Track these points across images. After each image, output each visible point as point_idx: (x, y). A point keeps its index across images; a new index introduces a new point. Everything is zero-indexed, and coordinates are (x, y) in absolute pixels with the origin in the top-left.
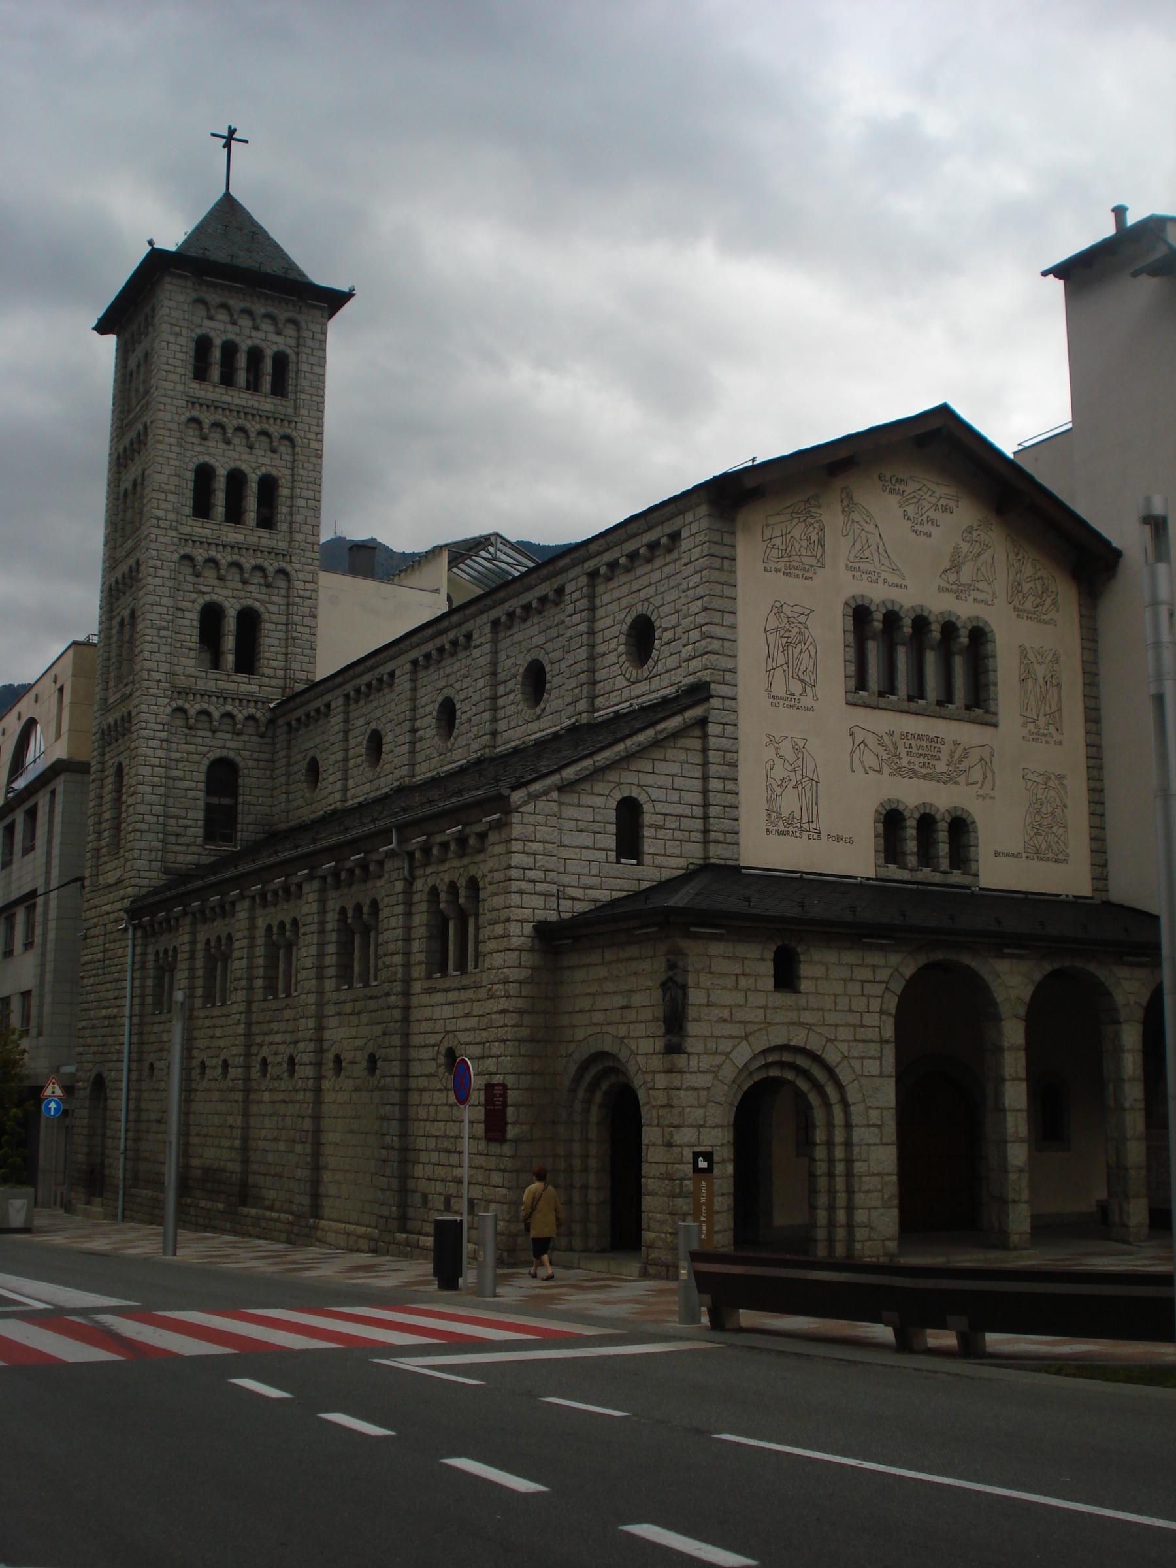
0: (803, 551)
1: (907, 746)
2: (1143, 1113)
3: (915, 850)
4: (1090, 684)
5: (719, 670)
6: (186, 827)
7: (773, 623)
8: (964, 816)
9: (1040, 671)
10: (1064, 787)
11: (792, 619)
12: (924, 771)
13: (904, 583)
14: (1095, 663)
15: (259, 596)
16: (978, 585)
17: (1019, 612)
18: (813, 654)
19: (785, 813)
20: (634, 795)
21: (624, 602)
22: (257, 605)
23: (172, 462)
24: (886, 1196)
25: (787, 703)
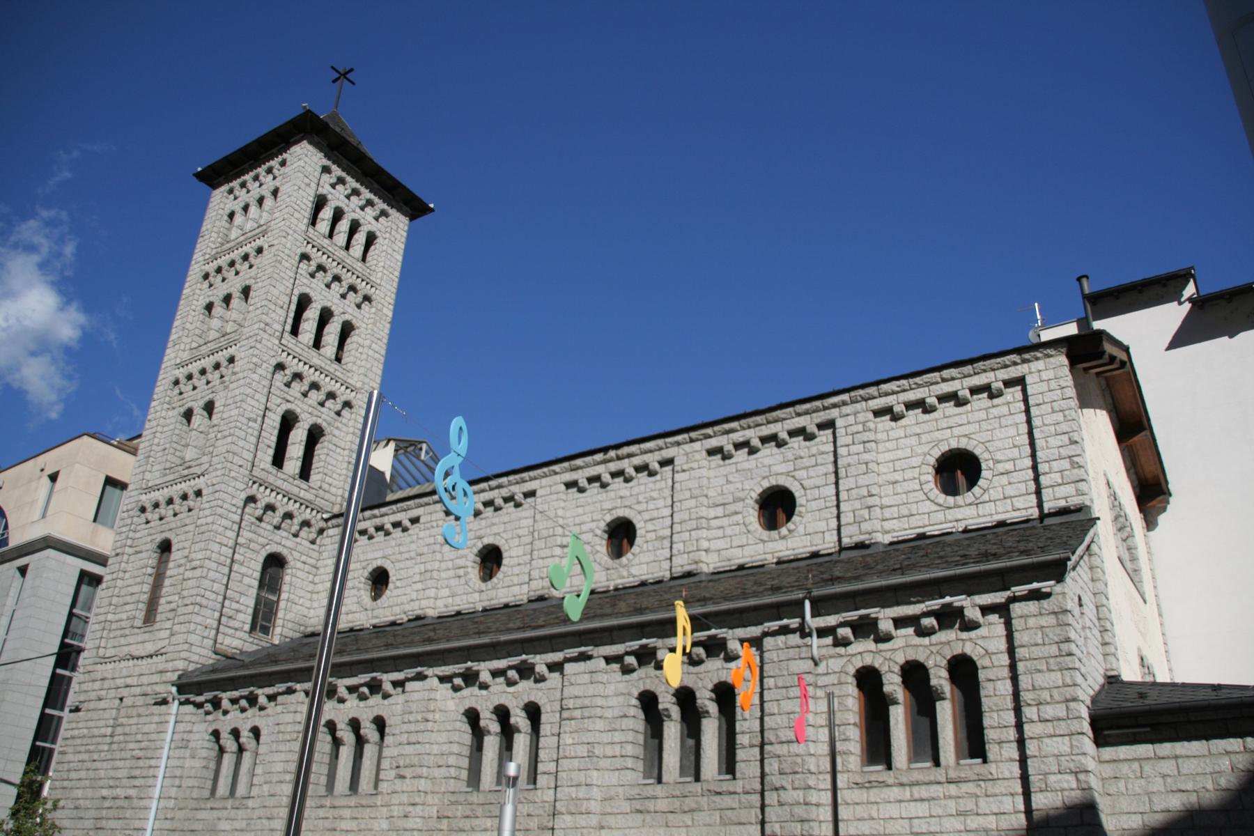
6: (238, 611)
15: (327, 418)
21: (925, 438)
22: (324, 425)
23: (284, 282)
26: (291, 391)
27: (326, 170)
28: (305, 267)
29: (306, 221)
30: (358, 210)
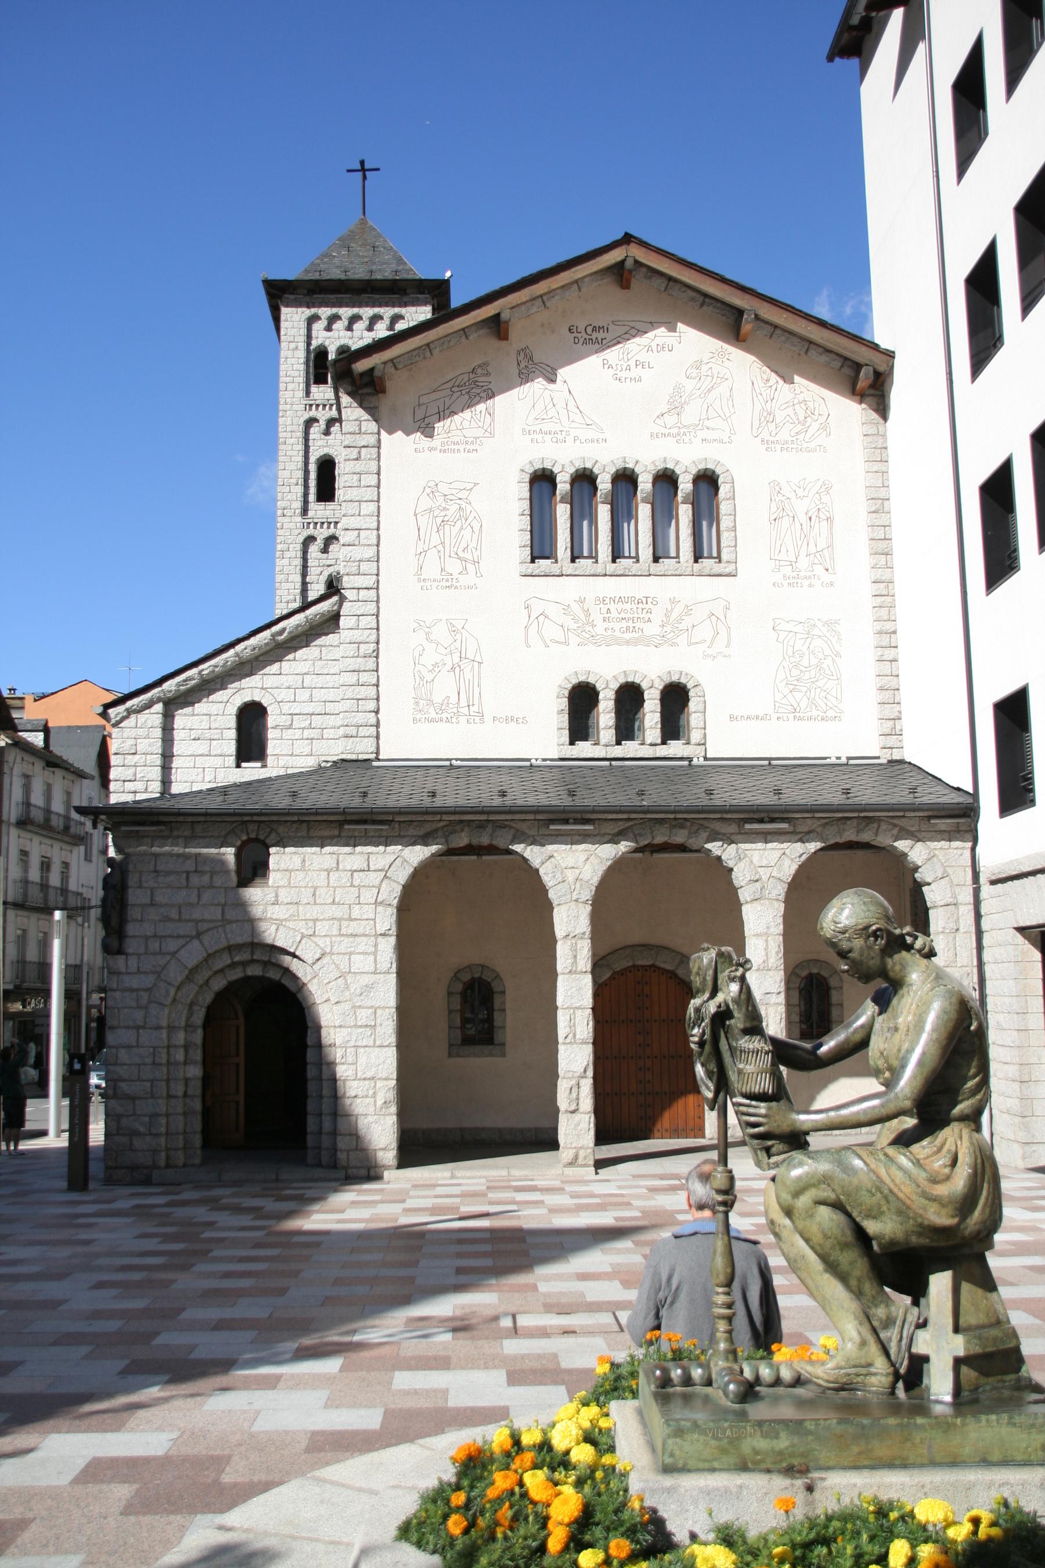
0: (466, 424)
1: (604, 610)
2: (782, 1009)
5: (354, 561)
7: (426, 503)
8: (683, 681)
9: (801, 507)
12: (628, 636)
13: (601, 436)
16: (707, 423)
18: (476, 529)
19: (437, 698)
20: (257, 699)
24: (379, 1103)
26: (331, 555)
27: (312, 320)
28: (317, 429)
29: (302, 386)
30: (366, 334)
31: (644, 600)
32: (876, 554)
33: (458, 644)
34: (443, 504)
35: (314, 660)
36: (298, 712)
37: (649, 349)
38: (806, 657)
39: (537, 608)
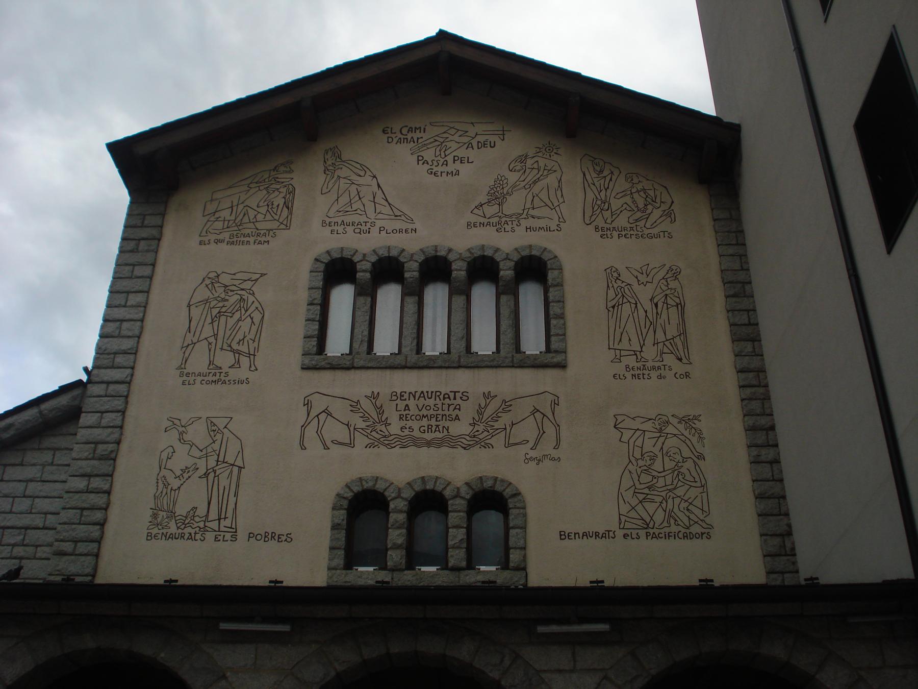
0: (260, 217)
3: (400, 541)
4: (734, 296)
5: (109, 354)
8: (498, 488)
9: (644, 294)
10: (700, 433)
11: (231, 288)
13: (410, 226)
14: (745, 269)
16: (532, 212)
17: (604, 233)
19: (181, 510)
25: (211, 378)
31: (452, 395)
32: (739, 340)
33: (216, 446)
34: (223, 296)
35: (44, 465)
36: (9, 524)
37: (470, 146)
38: (659, 462)
39: (319, 404)
